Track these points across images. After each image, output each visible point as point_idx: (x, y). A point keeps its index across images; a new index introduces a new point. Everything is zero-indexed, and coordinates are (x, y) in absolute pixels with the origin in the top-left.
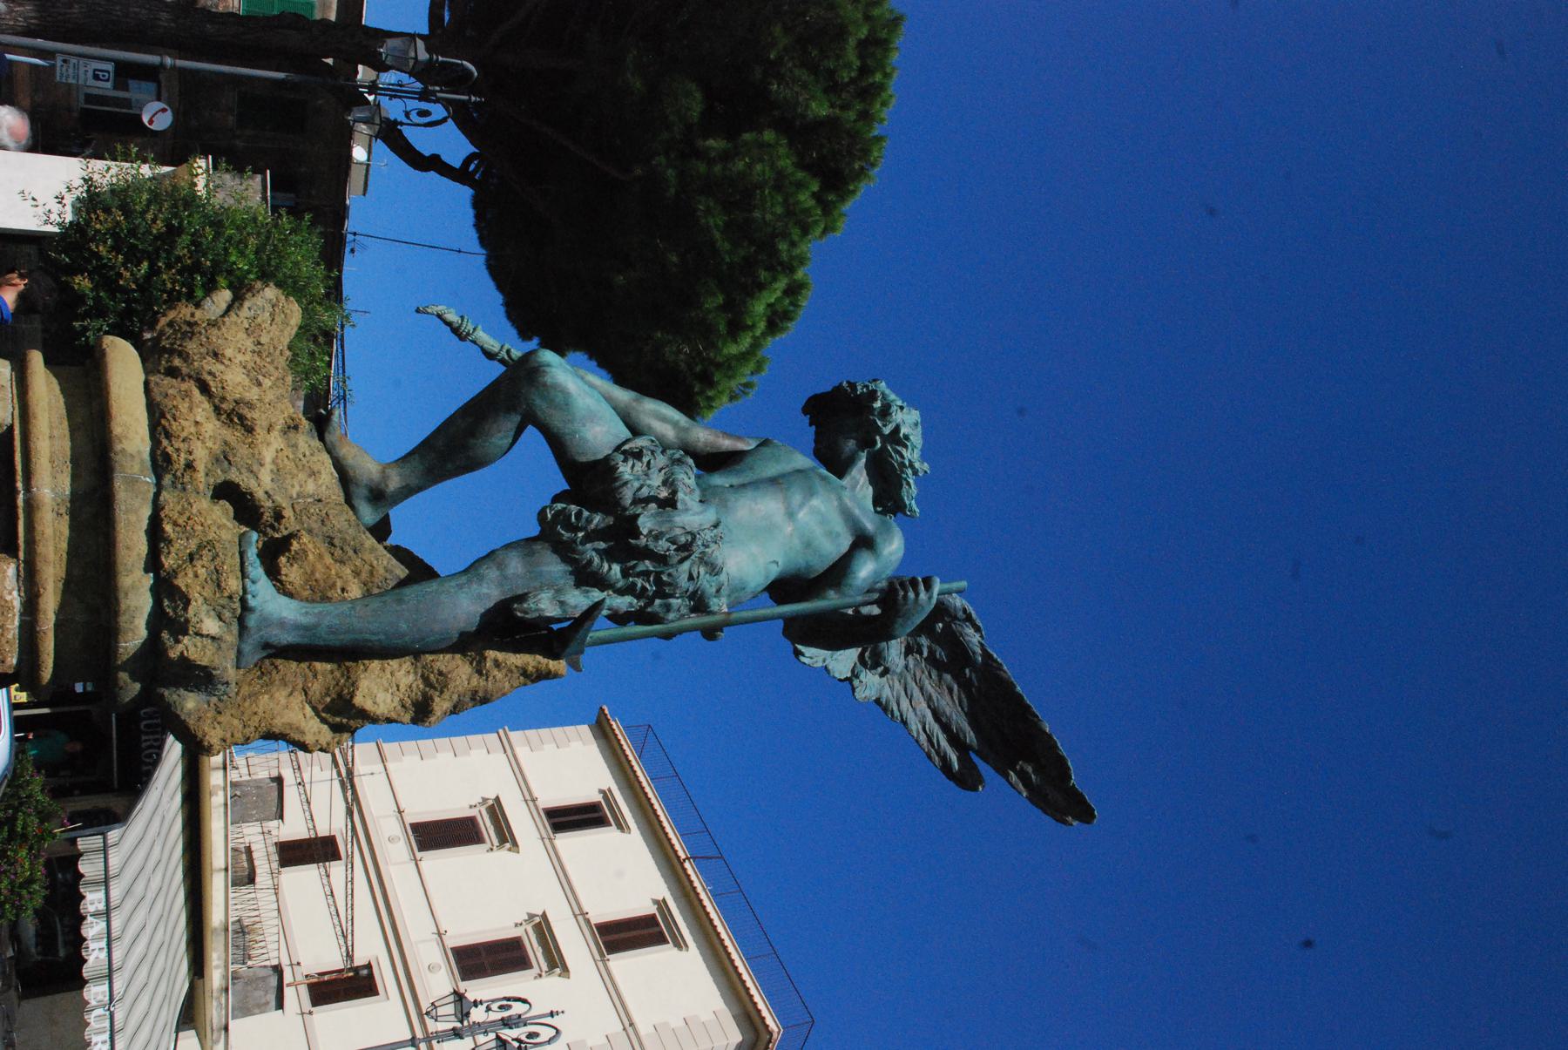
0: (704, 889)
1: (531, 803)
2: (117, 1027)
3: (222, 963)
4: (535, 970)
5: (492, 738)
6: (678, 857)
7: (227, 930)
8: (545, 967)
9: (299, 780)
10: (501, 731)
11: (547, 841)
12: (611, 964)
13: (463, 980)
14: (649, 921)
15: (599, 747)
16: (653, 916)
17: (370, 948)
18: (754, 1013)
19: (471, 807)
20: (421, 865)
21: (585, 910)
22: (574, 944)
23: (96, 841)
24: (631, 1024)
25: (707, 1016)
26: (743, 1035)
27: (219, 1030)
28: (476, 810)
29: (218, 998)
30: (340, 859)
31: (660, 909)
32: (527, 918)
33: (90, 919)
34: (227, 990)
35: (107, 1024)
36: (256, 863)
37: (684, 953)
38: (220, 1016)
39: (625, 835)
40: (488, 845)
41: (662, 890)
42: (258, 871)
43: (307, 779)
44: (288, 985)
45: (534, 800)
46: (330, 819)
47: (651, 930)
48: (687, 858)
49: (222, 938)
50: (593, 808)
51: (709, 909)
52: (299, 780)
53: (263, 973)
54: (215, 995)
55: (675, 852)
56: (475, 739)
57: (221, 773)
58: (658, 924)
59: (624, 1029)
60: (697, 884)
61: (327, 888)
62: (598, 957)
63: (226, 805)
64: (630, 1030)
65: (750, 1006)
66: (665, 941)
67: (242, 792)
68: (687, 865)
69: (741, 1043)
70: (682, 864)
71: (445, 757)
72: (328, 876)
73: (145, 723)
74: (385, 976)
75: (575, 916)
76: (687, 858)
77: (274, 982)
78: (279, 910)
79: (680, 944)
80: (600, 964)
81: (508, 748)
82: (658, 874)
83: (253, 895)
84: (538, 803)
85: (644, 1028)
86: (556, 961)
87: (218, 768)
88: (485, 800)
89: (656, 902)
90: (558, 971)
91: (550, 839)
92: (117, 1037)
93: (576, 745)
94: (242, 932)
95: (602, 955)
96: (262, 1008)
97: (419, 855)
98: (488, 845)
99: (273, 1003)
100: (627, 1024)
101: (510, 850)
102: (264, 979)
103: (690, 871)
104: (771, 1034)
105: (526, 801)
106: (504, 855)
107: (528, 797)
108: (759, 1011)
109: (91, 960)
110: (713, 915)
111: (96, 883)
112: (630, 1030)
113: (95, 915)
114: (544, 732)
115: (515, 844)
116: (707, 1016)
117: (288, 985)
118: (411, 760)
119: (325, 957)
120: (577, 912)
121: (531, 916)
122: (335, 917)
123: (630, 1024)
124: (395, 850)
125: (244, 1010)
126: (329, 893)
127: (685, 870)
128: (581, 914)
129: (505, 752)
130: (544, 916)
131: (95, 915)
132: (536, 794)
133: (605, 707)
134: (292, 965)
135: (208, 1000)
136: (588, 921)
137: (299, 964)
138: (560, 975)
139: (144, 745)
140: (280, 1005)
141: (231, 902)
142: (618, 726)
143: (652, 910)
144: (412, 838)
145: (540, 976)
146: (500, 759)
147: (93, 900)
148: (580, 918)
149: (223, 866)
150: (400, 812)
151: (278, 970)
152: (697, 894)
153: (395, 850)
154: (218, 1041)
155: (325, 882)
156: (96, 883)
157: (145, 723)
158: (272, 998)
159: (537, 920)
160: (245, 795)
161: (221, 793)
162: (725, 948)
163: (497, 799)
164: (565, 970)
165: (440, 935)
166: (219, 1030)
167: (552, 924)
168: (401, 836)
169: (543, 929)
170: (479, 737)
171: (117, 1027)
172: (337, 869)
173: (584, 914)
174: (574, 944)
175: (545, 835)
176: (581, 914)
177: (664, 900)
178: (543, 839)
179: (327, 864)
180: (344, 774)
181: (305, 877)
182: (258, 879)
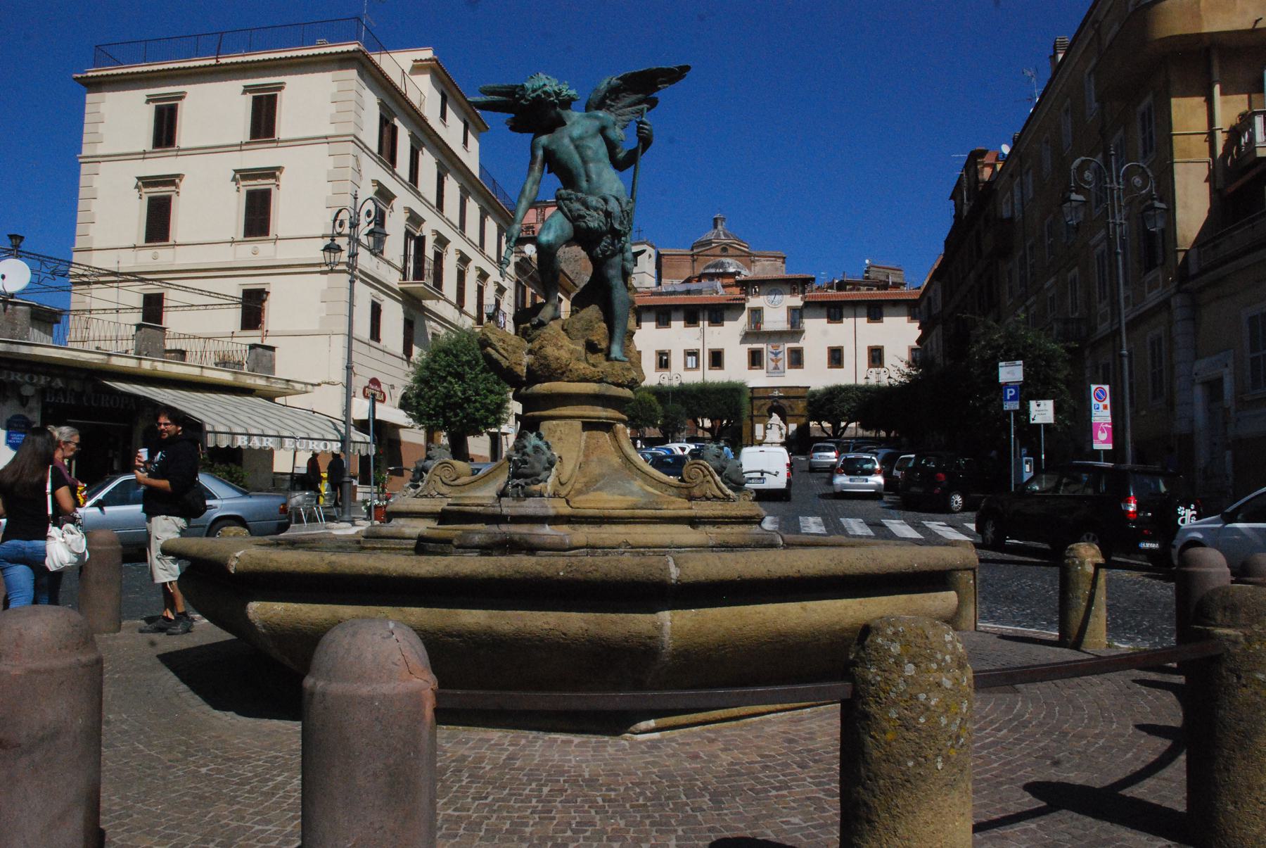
0: (244, 56)
1: (147, 156)
2: (307, 436)
3: (253, 378)
4: (273, 188)
5: (85, 169)
6: (215, 65)
7: (235, 373)
8: (273, 181)
9: (114, 311)
10: (80, 160)
11: (180, 153)
12: (282, 138)
13: (268, 235)
14: (256, 101)
15: (109, 91)
16: (254, 98)
17: (234, 287)
18: (342, 56)
19: (140, 198)
20: (178, 242)
21: (239, 142)
22: (261, 157)
23: (210, 437)
24: (326, 138)
25: (334, 88)
26: (352, 68)
27: (288, 385)
28: (143, 194)
29: (272, 383)
30: (162, 295)
31: (251, 92)
32: (234, 183)
33: (251, 445)
34: (268, 377)
35: (305, 441)
36: (173, 348)
37: (286, 87)
38: (280, 383)
39: (187, 97)
40: (174, 194)
41: (238, 85)
42: (178, 348)
43: (115, 306)
44: (262, 342)
45: (145, 152)
46: (133, 296)
47: (265, 103)
48: (217, 58)
49: (240, 376)
50: (160, 113)
51: (261, 57)
52: (114, 311)
53: (253, 356)
54: (269, 384)
55: (210, 66)
56: (83, 180)
57: (143, 362)
58: (262, 96)
59: (328, 143)
60: (240, 59)
61: (200, 308)
62: (275, 145)
63: (164, 362)
64: (329, 140)
65: (336, 56)
66: (275, 96)
67: (145, 350)
68: (223, 61)
69: (358, 72)
70: (221, 64)
71: (95, 206)
72: (193, 305)
73: (92, 402)
74: (254, 283)
75: (241, 150)
76: (217, 58)
77: (260, 350)
78: (209, 338)
79: (280, 87)
80: (280, 144)
81: (97, 159)
82: (223, 84)
83: (208, 353)
84: (147, 150)
85: (330, 131)
86: (272, 173)
87: (140, 363)
88: (137, 187)
89: (245, 92)
90: (277, 173)
91: (179, 150)
92: (312, 437)
93: (103, 108)
94: (224, 363)
95: (274, 141)
96: (272, 359)
97: (171, 242)
98: (174, 194)
99: (271, 352)
100: (325, 140)
101: (181, 180)
102: (257, 355)
103: (229, 60)
104: (359, 51)
105: (144, 158)
106: (183, 185)
107: (142, 156)
108: (342, 52)
109: (271, 446)
110: (266, 56)
111: (233, 439)
112: (329, 140)
113: (249, 441)
114: (87, 128)
115: (178, 176)
116: (334, 88)
117: (262, 342)
118: (92, 230)
119: (234, 316)
120: (239, 148)
121: (234, 179)
122: (223, 307)
123: (326, 138)
124: (163, 257)
125: (271, 369)
126: (204, 307)
127: (226, 64)
128: (241, 147)
129: (99, 162)
130: (236, 171)
131: (249, 441)
132: (141, 150)
133: (75, 75)
134: (232, 337)
135: (274, 389)
136: (247, 143)
137: (233, 333)
138: (281, 173)
139: (107, 406)
140: (272, 349)
141: (209, 366)
142: (93, 71)
143: (249, 97)
144: (157, 244)
145: (278, 185)
146: (103, 167)
147: (241, 442)
148: (244, 147)
149: (200, 369)
150: (135, 247)
151: (253, 347)
152: (247, 62)
153: (163, 257)
154: (293, 386)
155: (196, 308)
156: (233, 439)
157: (92, 402)
158: (268, 353)
159: (238, 176)
160: (146, 349)
161: (156, 364)
162: (292, 58)
163: (139, 179)
164: (279, 169)
165: (233, 242)
166: (288, 385)
167: (243, 168)
168: (154, 251)
169: (244, 175)
170: (82, 178)
171: (306, 436)
172: (172, 297)
173: (241, 144)
174: (261, 157)
175: (175, 153)
176: (241, 147)
177: (245, 86)
178: (177, 155)
179: (166, 303)
180: (116, 279)
181: (172, 320)
182: (184, 349)
